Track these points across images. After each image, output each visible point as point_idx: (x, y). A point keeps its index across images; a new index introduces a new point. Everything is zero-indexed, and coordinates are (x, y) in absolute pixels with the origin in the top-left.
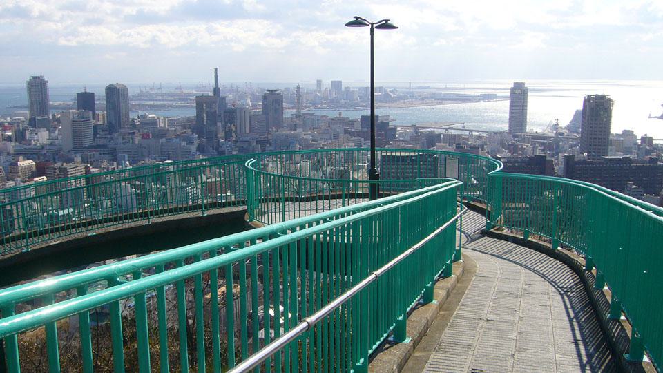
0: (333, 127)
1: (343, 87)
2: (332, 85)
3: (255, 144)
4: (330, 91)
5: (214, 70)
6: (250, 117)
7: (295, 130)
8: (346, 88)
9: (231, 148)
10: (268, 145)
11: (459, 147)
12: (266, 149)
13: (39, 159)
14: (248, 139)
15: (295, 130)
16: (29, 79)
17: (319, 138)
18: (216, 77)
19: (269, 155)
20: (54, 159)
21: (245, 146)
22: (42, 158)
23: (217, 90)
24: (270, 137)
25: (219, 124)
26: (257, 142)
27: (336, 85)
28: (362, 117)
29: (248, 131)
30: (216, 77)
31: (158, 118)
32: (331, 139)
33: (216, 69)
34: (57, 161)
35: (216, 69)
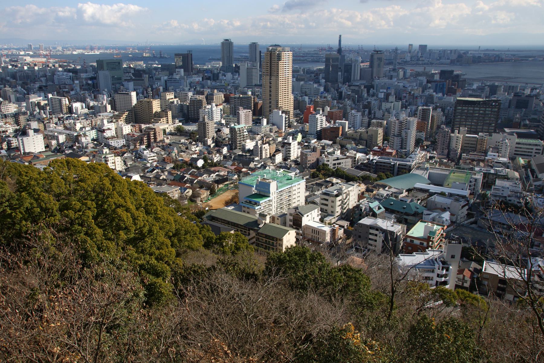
0: (420, 78)
1: (428, 49)
2: (419, 48)
3: (363, 88)
4: (418, 52)
5: (338, 36)
6: (361, 69)
7: (391, 79)
8: (430, 50)
9: (347, 90)
10: (372, 89)
11: (516, 95)
12: (371, 91)
13: (226, 92)
14: (358, 84)
15: (391, 79)
16: (222, 41)
17: (408, 85)
18: (340, 41)
19: (373, 96)
20: (235, 92)
21: (356, 88)
22: (228, 91)
23: (340, 50)
24: (373, 83)
25: (340, 73)
26: (365, 87)
27: (423, 48)
28: (441, 71)
29: (359, 78)
30: (340, 41)
31: (300, 68)
32: (417, 86)
33: (340, 36)
34: (236, 93)
35: (340, 36)
